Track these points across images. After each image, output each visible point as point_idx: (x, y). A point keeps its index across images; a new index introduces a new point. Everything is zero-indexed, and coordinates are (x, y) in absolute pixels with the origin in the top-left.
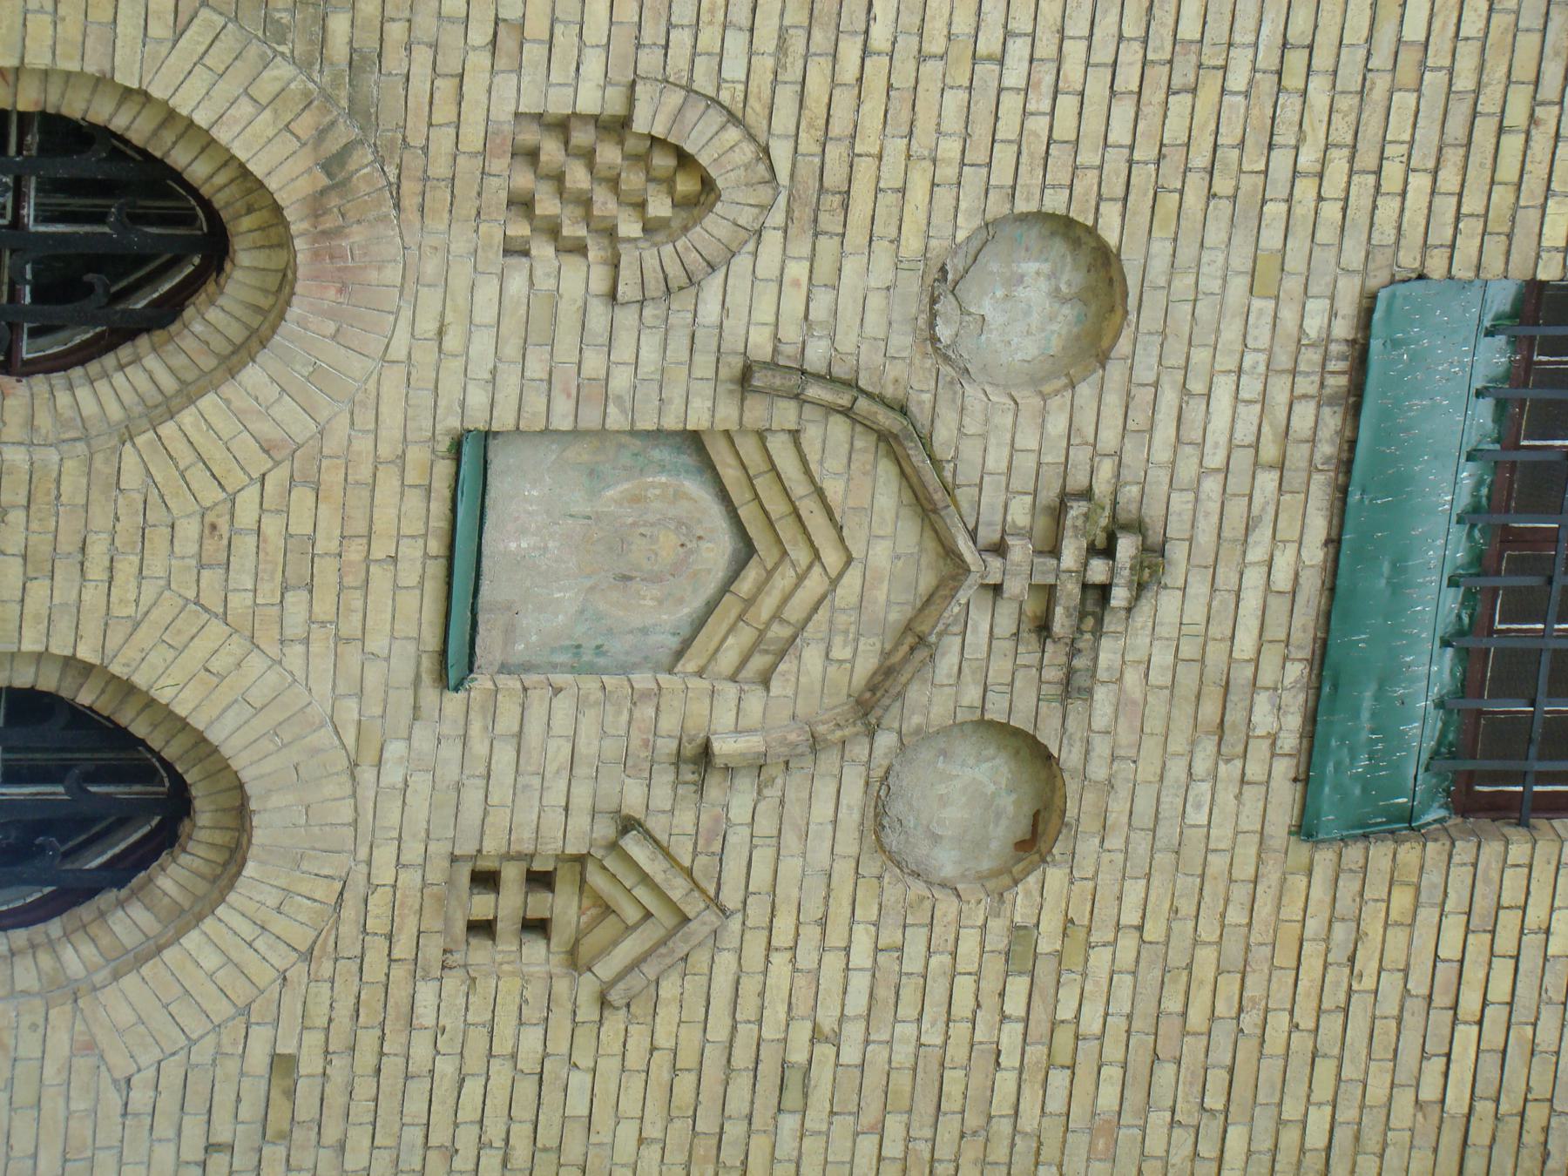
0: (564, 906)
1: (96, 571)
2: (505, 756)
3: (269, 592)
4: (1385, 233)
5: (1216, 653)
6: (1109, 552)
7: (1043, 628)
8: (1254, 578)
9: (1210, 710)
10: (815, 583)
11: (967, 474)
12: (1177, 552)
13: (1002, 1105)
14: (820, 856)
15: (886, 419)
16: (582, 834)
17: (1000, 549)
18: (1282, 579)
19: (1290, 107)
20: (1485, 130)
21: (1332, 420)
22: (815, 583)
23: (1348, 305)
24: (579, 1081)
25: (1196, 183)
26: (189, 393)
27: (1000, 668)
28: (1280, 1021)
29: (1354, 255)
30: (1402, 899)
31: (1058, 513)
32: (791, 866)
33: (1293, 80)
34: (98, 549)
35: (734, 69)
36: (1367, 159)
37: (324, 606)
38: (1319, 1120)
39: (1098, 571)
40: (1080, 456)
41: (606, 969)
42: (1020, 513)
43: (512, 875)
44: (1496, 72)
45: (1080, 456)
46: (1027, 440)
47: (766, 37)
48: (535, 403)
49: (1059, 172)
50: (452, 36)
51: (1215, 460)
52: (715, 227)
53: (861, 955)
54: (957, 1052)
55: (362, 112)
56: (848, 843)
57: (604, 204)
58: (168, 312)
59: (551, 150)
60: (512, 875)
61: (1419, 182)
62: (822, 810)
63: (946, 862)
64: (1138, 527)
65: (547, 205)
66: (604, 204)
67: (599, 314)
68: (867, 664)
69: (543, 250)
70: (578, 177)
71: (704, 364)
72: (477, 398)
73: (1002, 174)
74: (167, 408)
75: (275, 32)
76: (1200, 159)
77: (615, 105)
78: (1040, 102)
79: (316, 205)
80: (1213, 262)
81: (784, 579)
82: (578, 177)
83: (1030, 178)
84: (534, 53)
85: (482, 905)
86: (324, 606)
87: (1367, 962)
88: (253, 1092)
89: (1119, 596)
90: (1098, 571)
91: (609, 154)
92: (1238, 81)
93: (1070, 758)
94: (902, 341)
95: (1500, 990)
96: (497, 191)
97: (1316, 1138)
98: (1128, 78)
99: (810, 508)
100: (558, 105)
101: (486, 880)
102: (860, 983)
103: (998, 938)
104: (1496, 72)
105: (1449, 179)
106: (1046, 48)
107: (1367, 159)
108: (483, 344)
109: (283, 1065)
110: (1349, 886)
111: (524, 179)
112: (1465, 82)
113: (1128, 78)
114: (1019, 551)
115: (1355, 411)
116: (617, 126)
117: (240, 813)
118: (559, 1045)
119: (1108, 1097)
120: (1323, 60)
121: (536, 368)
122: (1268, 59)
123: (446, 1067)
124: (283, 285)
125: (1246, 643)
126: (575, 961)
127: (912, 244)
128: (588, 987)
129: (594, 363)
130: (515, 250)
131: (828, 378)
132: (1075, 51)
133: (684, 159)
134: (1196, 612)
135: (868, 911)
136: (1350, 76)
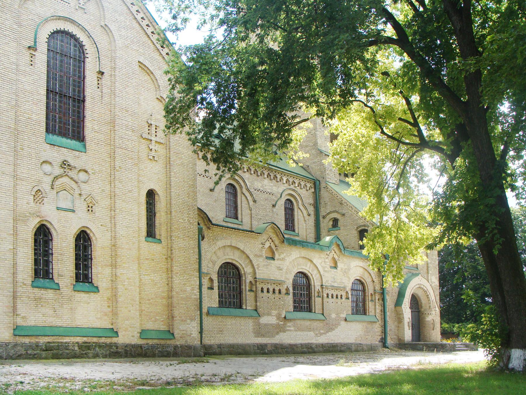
0: (90, 205)
1: (67, 235)
2: (80, 208)
3: (68, 224)
4: (42, 142)
5: (73, 157)
6: (65, 164)
7: (71, 169)
8: (67, 154)
9: (77, 158)
10: (67, 185)
11: (60, 173)
12: (65, 159)
13: (105, 176)
14: (87, 187)
15: (56, 179)
16: (85, 203)
17: (65, 172)
18: (67, 152)
19: (33, 147)
20: (34, 134)
21: (55, 147)
22: (67, 185)
23: (47, 145)
24: (103, 205)
25: (38, 155)
26: (54, 228)
27: (74, 173)
28: (99, 156)
29: (43, 144)
30: (90, 146)
31: (63, 167)
32: (88, 189)
33: (31, 147)
34: (66, 235)
35: (30, 187)
36: (36, 142)
37: (69, 220)
38: (106, 154)
39: (67, 165)
40: (58, 165)
41: (95, 203)
42: (62, 170)
43: (88, 209)
44: (30, 132)
45: (58, 165)
46: (57, 169)
47: (28, 185)
48: (54, 204)
49: (37, 165)
50: (28, 207)
51: (58, 156)
52: (41, 190)
53: (94, 185)
54: (101, 179)
55: (34, 214)
56: (86, 185)
57: (40, 197)
58: (48, 229)
59: (36, 201)
60: (88, 209)
61: (38, 139)
62: (84, 186)
63: (87, 178)
64: (63, 162)
65: (40, 201)
66: (40, 197)
67: (48, 198)
68: (73, 182)
69: (43, 202)
70: (38, 199)
71: (51, 191)
72: (54, 208)
73: (38, 169)
74: (55, 230)
75: (28, 219)
76: (36, 154)
77: (33, 196)
78: (32, 165)
79: (40, 218)
80: (44, 154)
81: (67, 187)
82: (38, 199)
83: (38, 167)
84: (29, 201)
85: (90, 211)
86: (69, 220)
87: (95, 149)
88: (103, 227)
89: (69, 164)
90: (67, 165)
91: (36, 197)
92: (31, 151)
93: (80, 168)
94: (50, 177)
95: (97, 140)
96: (39, 205)
97: (107, 154)
98: (31, 159)
99: (62, 185)
100: (33, 200)
101: (88, 210)
102: (96, 185)
103: (93, 175)
104: (30, 132)
105: (38, 137)
106: (28, 164)
107: (36, 142)
108: (50, 207)
109: (101, 225)
110: (89, 150)
111: (38, 203)
112: (31, 135)
113: (31, 159)
114: (65, 170)
115: (55, 145)
116: (34, 196)
117: (84, 227)
118: (100, 206)
119: (104, 168)
120: (29, 145)
121: (52, 203)
122: (29, 149)
123: (102, 214)
124: (46, 221)
125: (72, 155)
126: (94, 205)
127: (43, 176)
128: (96, 204)
129: (52, 199)
130: (43, 204)
131: (53, 183)
132: (28, 162)
133: (37, 191)
134: (69, 158)
135: (91, 184)
136: (31, 143)
